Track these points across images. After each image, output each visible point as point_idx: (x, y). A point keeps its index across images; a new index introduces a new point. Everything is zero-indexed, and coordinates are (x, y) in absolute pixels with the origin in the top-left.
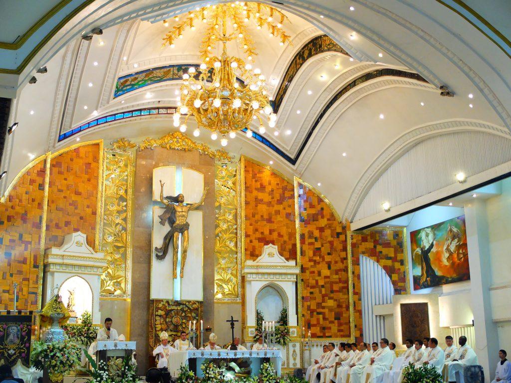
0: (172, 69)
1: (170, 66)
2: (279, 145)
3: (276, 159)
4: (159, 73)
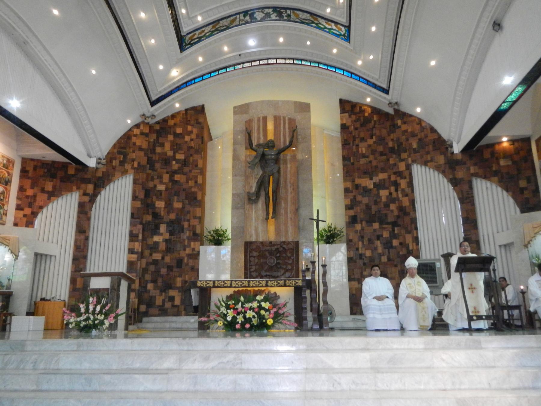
0: (238, 16)
1: (236, 14)
4: (225, 22)
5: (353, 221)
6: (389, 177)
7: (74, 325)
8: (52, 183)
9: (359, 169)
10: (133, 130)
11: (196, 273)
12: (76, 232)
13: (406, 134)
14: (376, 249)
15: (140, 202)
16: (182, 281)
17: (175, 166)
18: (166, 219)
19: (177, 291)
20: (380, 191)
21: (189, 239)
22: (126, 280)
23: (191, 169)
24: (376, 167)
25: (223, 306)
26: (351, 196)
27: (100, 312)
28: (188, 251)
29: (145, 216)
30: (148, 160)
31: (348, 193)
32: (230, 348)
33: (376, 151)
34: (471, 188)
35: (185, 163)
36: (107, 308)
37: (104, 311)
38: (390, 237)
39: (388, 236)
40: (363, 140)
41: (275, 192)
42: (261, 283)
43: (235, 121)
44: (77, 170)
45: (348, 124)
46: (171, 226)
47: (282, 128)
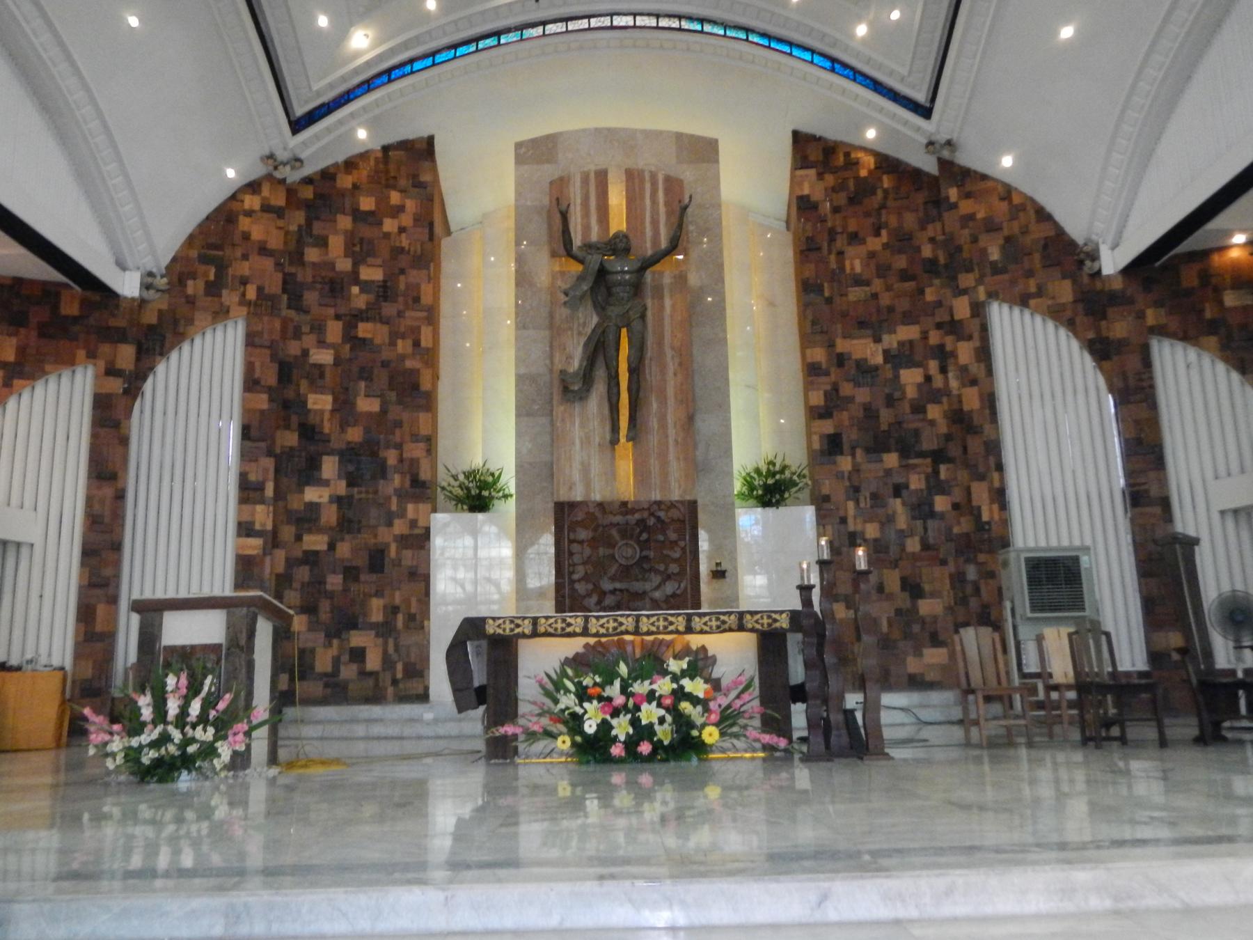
2: (880, 67)
3: (887, 121)
5: (833, 445)
6: (925, 336)
7: (120, 759)
8: (14, 340)
9: (844, 315)
10: (240, 196)
11: (423, 584)
12: (90, 477)
13: (971, 224)
14: (891, 519)
15: (265, 397)
16: (385, 607)
17: (358, 298)
18: (336, 444)
19: (373, 632)
20: (903, 372)
21: (402, 495)
22: (268, 619)
23: (401, 307)
24: (891, 309)
25: (567, 691)
26: (825, 383)
27: (203, 719)
28: (399, 527)
29: (281, 436)
30: (285, 282)
31: (818, 375)
32: (832, 916)
33: (889, 268)
34: (1147, 363)
35: (385, 292)
36: (222, 706)
37: (213, 714)
38: (929, 488)
39: (923, 486)
40: (855, 238)
41: (635, 371)
42: (671, 623)
43: (519, 184)
44: (84, 303)
45: (814, 198)
46: (350, 461)
47: (648, 202)
